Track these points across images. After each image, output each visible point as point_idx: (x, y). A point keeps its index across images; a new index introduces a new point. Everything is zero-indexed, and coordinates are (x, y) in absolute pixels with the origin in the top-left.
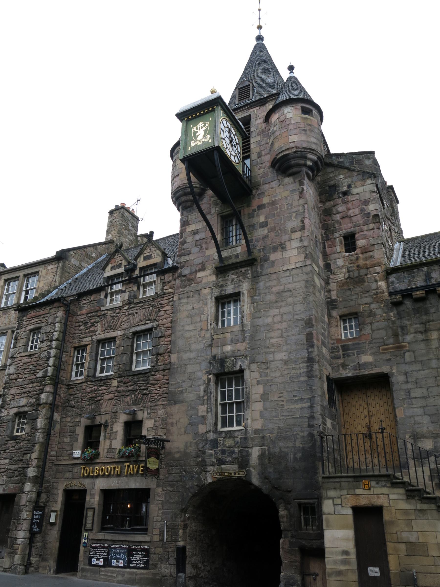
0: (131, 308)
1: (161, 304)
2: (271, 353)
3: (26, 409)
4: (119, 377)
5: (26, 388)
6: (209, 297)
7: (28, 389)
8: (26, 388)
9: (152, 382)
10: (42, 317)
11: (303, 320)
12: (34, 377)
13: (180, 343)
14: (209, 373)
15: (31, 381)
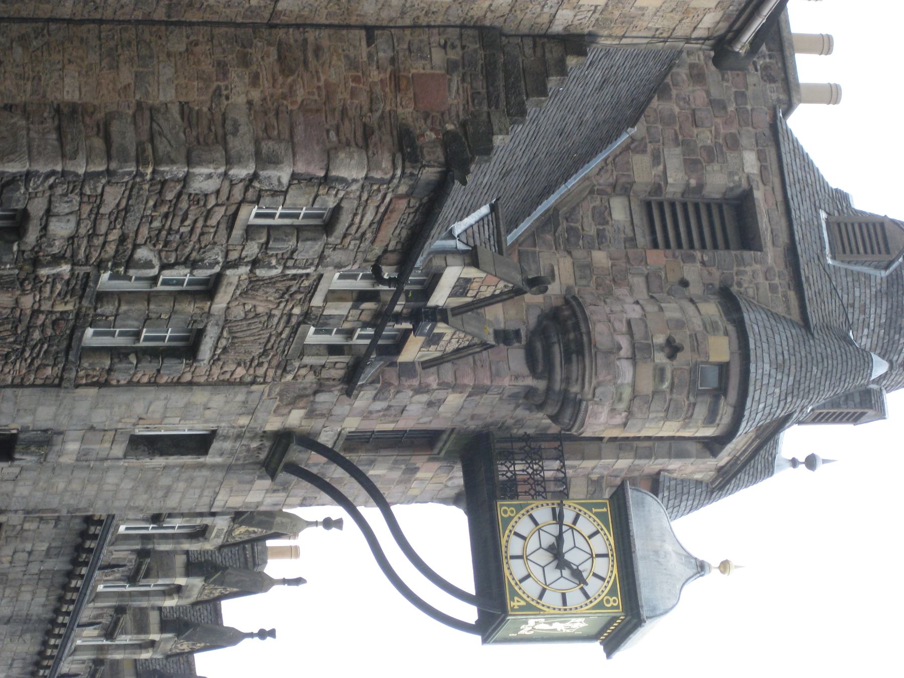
0: (290, 315)
1: (260, 364)
2: (35, 483)
3: (32, 236)
4: (77, 315)
5: (110, 229)
6: (223, 424)
7: (103, 227)
8: (110, 229)
9: (37, 363)
10: (369, 235)
11: (91, 505)
12: (140, 240)
13: (124, 397)
14: (25, 430)
15: (132, 235)
